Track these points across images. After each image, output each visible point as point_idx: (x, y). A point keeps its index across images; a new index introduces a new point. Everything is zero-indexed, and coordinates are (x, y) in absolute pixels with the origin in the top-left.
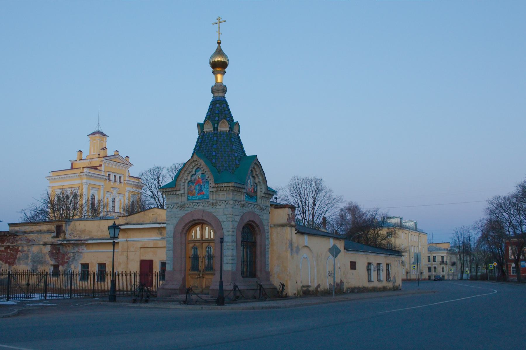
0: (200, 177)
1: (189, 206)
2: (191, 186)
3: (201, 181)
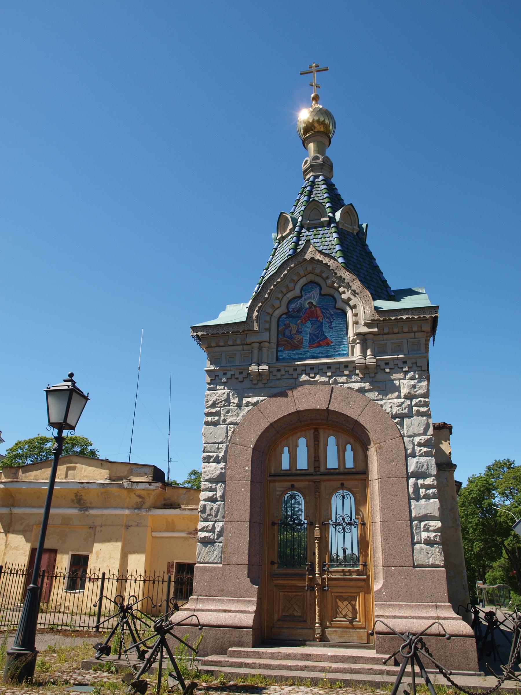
0: (314, 303)
1: (281, 375)
2: (287, 327)
3: (319, 312)
